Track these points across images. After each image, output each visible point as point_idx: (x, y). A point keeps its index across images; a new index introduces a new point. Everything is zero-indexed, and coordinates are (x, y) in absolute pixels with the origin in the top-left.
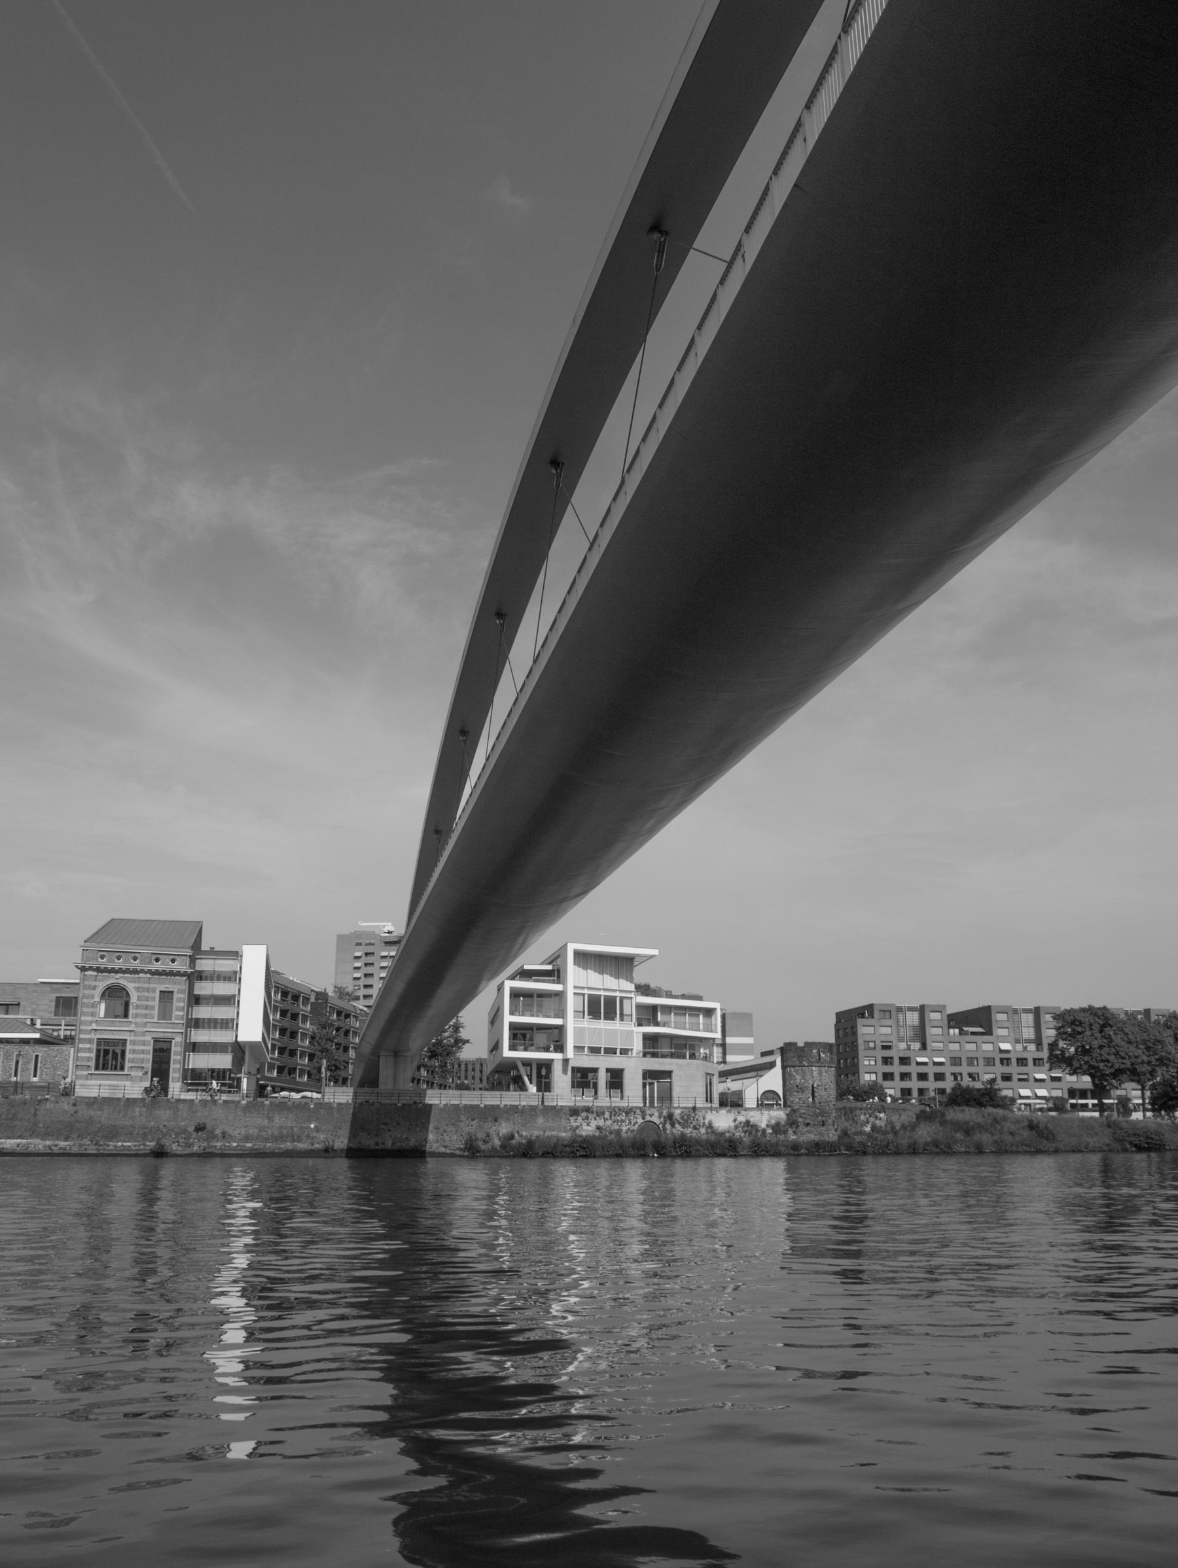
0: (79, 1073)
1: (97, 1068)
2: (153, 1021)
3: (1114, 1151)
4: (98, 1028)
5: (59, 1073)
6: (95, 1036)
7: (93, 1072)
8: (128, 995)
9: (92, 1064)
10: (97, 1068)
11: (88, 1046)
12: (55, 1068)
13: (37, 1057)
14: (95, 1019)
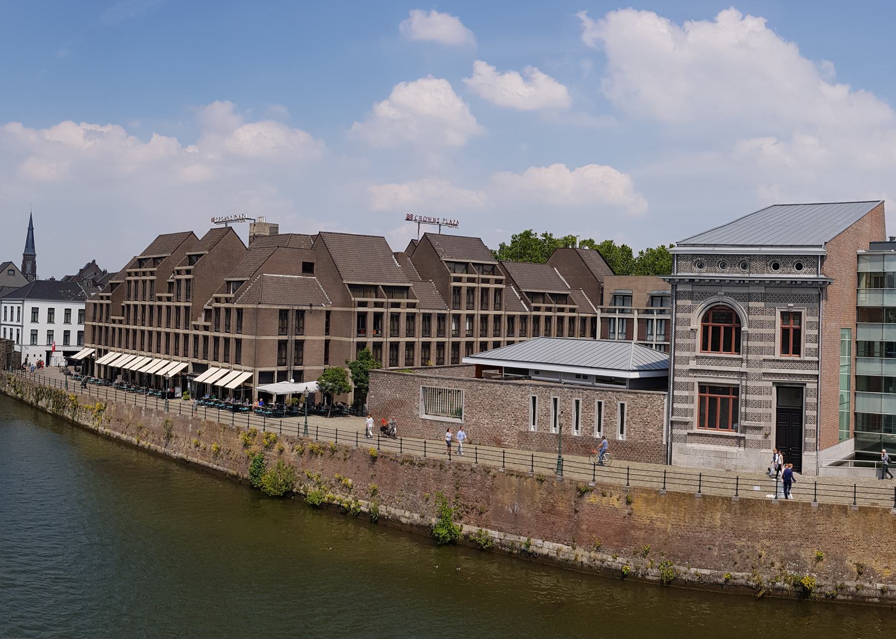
0: (676, 431)
1: (701, 424)
2: (772, 357)
3: (588, 491)
4: (699, 367)
5: (651, 430)
6: (696, 380)
7: (696, 430)
8: (739, 321)
9: (695, 419)
10: (701, 424)
11: (686, 393)
12: (646, 424)
13: (622, 405)
14: (694, 354)
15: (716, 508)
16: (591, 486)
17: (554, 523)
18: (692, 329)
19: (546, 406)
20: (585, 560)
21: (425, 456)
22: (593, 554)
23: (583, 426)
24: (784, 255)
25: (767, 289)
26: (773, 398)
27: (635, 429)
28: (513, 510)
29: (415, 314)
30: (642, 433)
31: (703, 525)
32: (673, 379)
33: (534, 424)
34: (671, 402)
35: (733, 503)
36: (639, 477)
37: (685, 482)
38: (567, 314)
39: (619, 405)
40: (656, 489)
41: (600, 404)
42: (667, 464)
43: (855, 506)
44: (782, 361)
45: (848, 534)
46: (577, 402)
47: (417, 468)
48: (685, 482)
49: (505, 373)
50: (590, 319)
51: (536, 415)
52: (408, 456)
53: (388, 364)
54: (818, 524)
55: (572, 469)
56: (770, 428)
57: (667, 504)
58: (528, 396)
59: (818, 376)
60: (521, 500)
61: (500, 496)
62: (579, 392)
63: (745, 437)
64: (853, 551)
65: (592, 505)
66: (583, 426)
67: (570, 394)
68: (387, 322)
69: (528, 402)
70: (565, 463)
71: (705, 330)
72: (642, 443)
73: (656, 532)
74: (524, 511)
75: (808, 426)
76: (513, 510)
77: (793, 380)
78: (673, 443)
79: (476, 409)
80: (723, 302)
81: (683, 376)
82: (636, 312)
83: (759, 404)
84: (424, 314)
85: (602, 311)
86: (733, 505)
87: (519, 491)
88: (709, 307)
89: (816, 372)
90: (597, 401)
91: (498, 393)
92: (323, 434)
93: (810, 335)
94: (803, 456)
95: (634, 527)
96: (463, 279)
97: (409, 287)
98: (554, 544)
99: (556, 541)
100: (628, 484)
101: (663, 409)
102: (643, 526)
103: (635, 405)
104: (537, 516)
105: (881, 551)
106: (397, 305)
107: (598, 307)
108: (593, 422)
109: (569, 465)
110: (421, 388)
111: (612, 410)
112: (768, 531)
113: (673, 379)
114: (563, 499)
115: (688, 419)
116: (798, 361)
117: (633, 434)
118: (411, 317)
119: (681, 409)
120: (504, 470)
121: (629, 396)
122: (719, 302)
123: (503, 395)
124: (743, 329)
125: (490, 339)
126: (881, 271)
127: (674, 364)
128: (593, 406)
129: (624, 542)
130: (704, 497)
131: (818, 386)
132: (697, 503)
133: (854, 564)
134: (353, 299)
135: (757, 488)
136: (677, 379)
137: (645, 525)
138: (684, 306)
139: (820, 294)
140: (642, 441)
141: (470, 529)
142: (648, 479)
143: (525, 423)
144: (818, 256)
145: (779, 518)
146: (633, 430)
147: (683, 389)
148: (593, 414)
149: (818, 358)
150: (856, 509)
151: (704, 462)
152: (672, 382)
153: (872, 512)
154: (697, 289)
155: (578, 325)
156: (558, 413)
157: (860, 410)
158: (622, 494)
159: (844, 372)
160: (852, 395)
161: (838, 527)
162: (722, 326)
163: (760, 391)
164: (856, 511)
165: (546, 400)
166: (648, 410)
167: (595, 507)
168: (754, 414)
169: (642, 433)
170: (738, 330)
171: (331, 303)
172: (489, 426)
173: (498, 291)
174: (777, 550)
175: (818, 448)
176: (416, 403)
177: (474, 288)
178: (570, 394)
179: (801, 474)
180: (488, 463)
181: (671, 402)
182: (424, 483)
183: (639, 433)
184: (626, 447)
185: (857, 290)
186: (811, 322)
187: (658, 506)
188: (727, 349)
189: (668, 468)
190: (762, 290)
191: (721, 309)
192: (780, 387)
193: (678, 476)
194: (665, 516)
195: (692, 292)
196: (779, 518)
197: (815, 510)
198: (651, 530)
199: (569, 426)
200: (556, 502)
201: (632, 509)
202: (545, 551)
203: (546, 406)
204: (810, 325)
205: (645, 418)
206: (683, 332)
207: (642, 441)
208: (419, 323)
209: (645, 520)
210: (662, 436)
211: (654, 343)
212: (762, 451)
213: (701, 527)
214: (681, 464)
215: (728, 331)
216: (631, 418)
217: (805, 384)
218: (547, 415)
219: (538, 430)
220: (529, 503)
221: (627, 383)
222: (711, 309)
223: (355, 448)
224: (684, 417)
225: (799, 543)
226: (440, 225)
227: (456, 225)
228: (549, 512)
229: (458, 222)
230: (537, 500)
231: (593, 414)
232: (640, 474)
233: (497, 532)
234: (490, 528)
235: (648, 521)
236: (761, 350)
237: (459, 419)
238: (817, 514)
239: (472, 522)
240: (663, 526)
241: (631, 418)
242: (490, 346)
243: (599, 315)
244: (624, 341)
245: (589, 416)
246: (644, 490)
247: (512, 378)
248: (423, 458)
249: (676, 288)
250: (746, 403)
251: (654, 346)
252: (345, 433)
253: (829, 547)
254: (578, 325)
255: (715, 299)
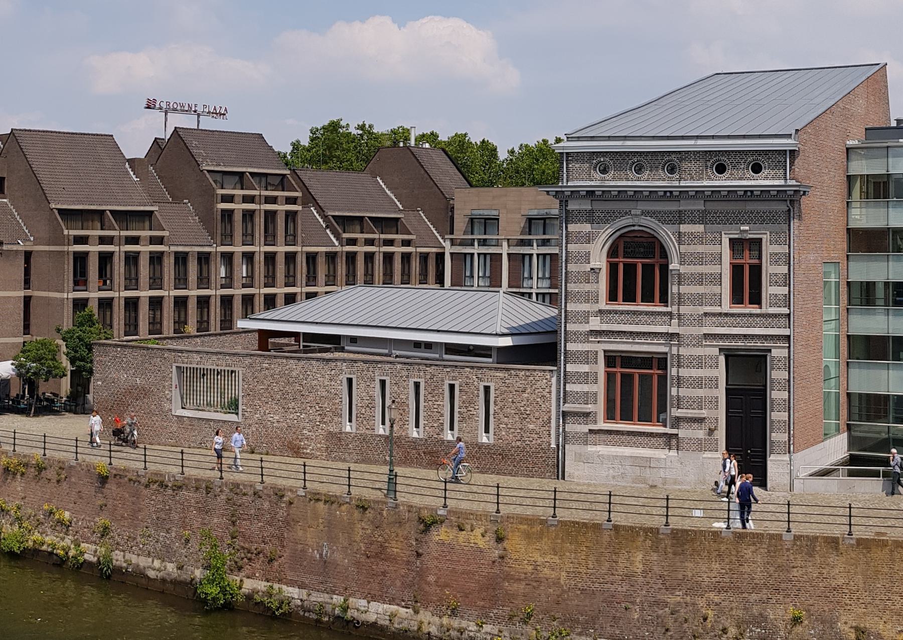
1: (610, 415)
2: (717, 309)
3: (436, 522)
4: (605, 327)
5: (531, 426)
6: (600, 347)
7: (602, 425)
8: (664, 254)
9: (600, 408)
10: (610, 415)
11: (585, 368)
12: (524, 417)
13: (487, 389)
14: (596, 308)
15: (635, 546)
16: (441, 515)
17: (384, 573)
18: (592, 269)
19: (368, 393)
20: (433, 630)
21: (183, 473)
22: (445, 620)
23: (426, 422)
24: (733, 151)
25: (708, 204)
26: (720, 372)
27: (506, 424)
28: (321, 555)
29: (162, 253)
30: (519, 431)
31: (615, 572)
32: (565, 347)
33: (350, 421)
34: (562, 382)
35: (661, 536)
36: (514, 499)
37: (587, 506)
38: (398, 249)
39: (482, 389)
40: (542, 518)
41: (452, 387)
42: (558, 479)
43: (851, 538)
44: (732, 315)
45: (841, 581)
46: (417, 385)
47: (170, 492)
48: (587, 506)
49: (304, 342)
50: (434, 256)
51: (354, 407)
52: (156, 474)
53: (122, 332)
54: (793, 567)
55: (411, 490)
56: (717, 419)
57: (559, 541)
58: (341, 377)
59: (789, 337)
60: (332, 539)
61: (300, 533)
62: (419, 370)
63: (677, 435)
64: (849, 607)
65: (444, 544)
66: (426, 422)
67: (404, 373)
68: (119, 267)
69: (340, 387)
70: (399, 480)
71: (613, 269)
72: (518, 447)
73: (543, 584)
74: (338, 556)
75: (776, 416)
76: (321, 555)
77: (751, 344)
78: (567, 446)
79: (259, 399)
80: (640, 226)
81: (581, 342)
82: (505, 244)
83: (699, 383)
84: (176, 253)
85: (453, 242)
86: (661, 539)
87: (330, 524)
88: (618, 234)
89: (786, 332)
90: (447, 382)
91: (294, 374)
92: (23, 443)
93: (776, 275)
94: (769, 463)
95: (508, 577)
96: (236, 199)
97: (152, 212)
98: (385, 606)
99: (389, 601)
100: (498, 511)
101: (550, 392)
102: (523, 576)
103: (506, 389)
104: (358, 563)
105: (893, 607)
106: (135, 240)
107: (446, 237)
108: (442, 415)
109: (407, 483)
110: (174, 367)
111: (472, 396)
112: (717, 580)
113: (565, 347)
114: (397, 536)
115: (590, 408)
116: (758, 315)
117: (504, 433)
118: (156, 259)
119: (577, 393)
120: (305, 492)
121: (498, 374)
122: (634, 226)
123: (301, 376)
124: (671, 267)
125: (281, 290)
126: (884, 172)
127: (566, 323)
128: (441, 390)
129: (494, 601)
130: (616, 528)
131: (789, 352)
132: (606, 538)
133: (851, 627)
134: (66, 232)
135: (698, 513)
136: (571, 347)
137: (526, 574)
138: (579, 233)
139: (789, 210)
140: (518, 443)
141: (255, 586)
142: (528, 501)
143: (336, 419)
144: (786, 151)
145: (734, 558)
146: (504, 426)
147: (581, 362)
148: (441, 403)
149: (789, 309)
150: (852, 542)
151: (614, 474)
152: (563, 351)
153: (878, 546)
154: (599, 206)
155: (415, 265)
156: (388, 402)
157: (854, 389)
158: (489, 527)
159: (830, 331)
160: (843, 367)
161: (824, 571)
162: (639, 262)
163: (700, 363)
164: (852, 546)
165: (368, 384)
166: (526, 395)
167: (448, 548)
168: (691, 398)
169: (519, 431)
170: (665, 269)
171: (32, 239)
172: (281, 425)
173: (291, 216)
174: (732, 609)
175: (792, 448)
176: (167, 392)
177: (254, 211)
178: (404, 373)
179: (767, 490)
180: (281, 483)
181: (562, 382)
182: (182, 515)
183: (513, 430)
184: (494, 454)
185: (848, 203)
186: (776, 254)
187: (545, 544)
188: (648, 298)
189: (560, 485)
190: (700, 206)
191: (637, 237)
192: (731, 356)
193: (575, 496)
194: (556, 559)
195: (592, 211)
196: (734, 558)
197: (788, 545)
198: (535, 581)
199: (405, 423)
200: (386, 541)
201: (505, 549)
202: (371, 618)
203: (368, 393)
204: (776, 259)
205: (522, 408)
206: (579, 273)
207: (518, 443)
208: (169, 267)
209: (526, 566)
210: (549, 435)
211: (534, 291)
212: (705, 456)
213: (613, 574)
214: (580, 479)
215: (648, 270)
216: (501, 409)
217: (770, 351)
218: (372, 407)
219: (357, 429)
220: (346, 544)
221: (494, 354)
222: (621, 236)
223: (73, 463)
224: (583, 406)
225: (765, 597)
226: (199, 115)
227: (224, 114)
228: (377, 555)
229: (226, 110)
230: (358, 539)
231: (441, 403)
232: (515, 494)
233: (297, 590)
234: (286, 584)
235: (530, 568)
236: (700, 300)
237: (234, 415)
238: (791, 551)
239: (257, 575)
240: (554, 575)
241: (501, 409)
242: (280, 300)
243: (448, 249)
244: (487, 289)
245: (435, 406)
246: (523, 520)
247: (316, 349)
248: (179, 477)
249: (567, 206)
250: (679, 381)
251: (534, 296)
252: (58, 441)
253: (811, 602)
254: (415, 265)
255: (628, 221)
